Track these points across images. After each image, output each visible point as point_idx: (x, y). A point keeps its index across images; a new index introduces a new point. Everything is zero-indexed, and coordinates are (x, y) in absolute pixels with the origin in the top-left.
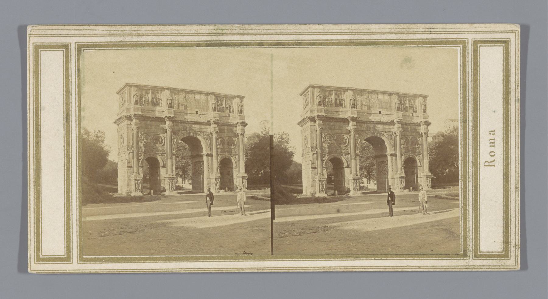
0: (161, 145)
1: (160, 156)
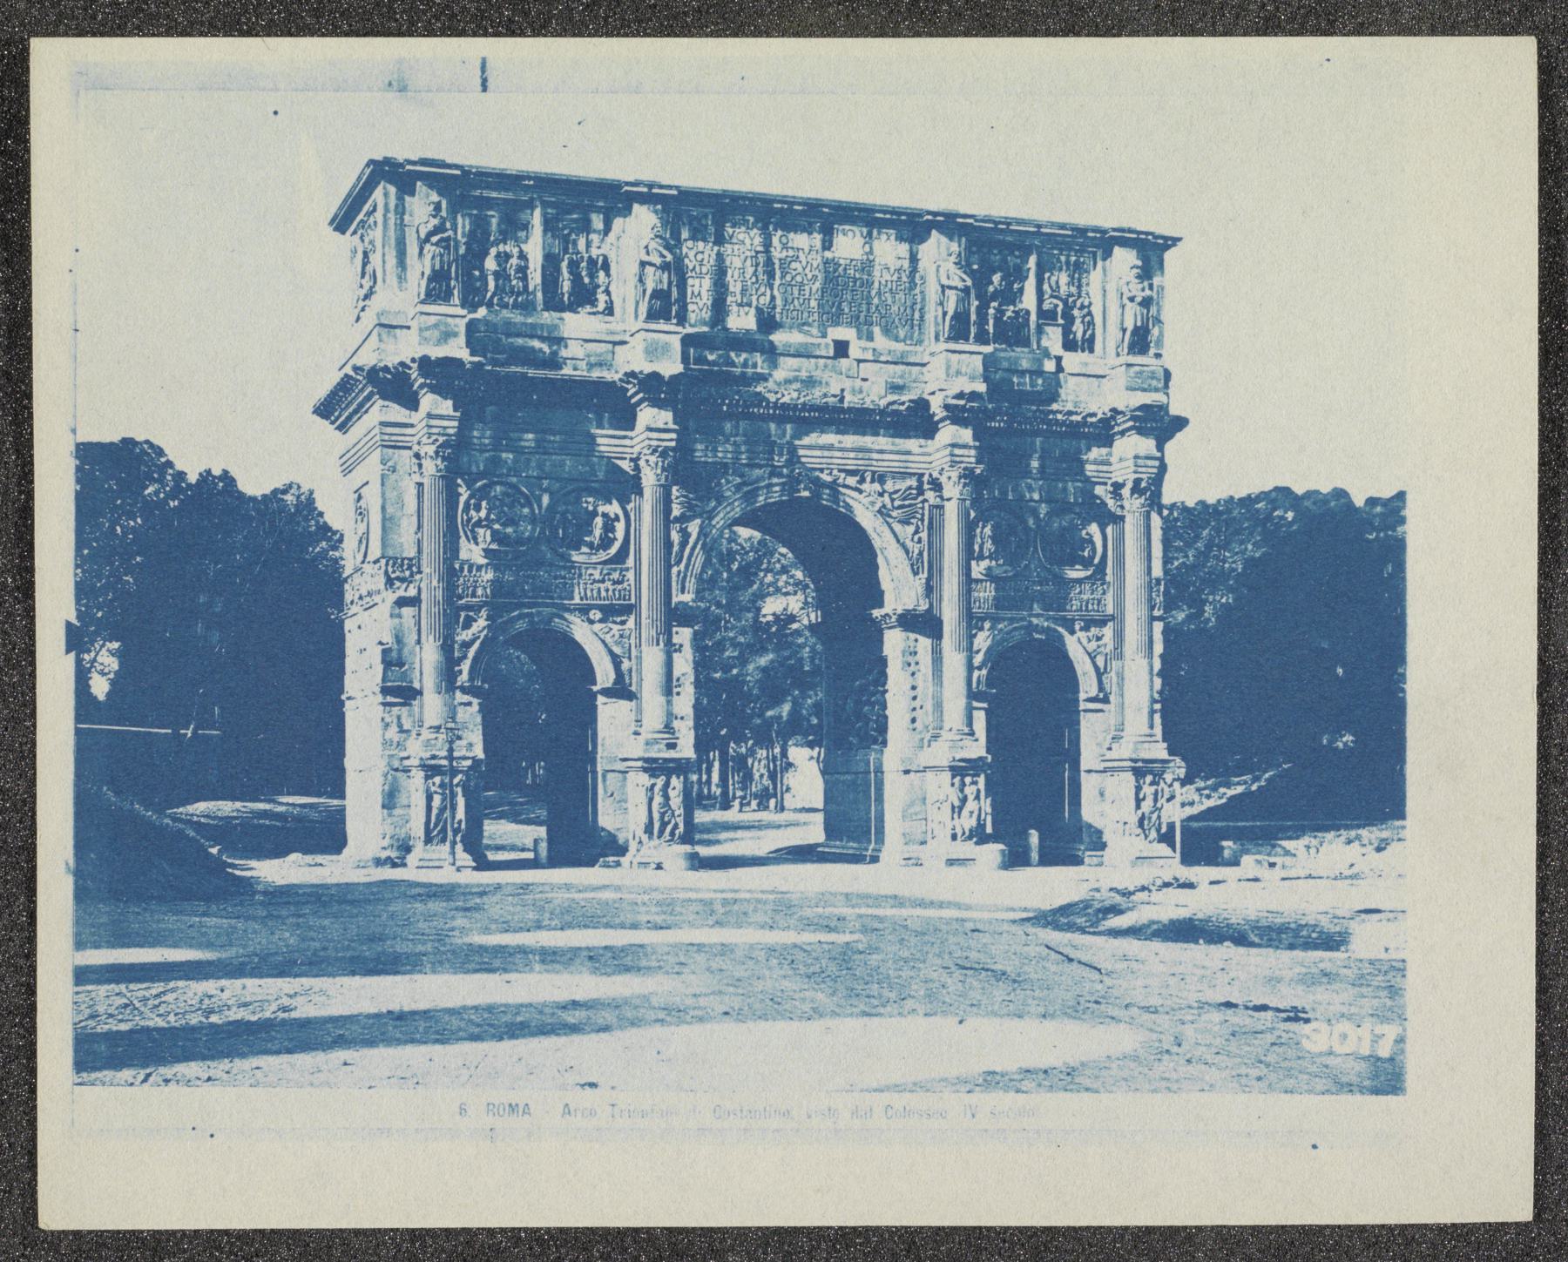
0: (603, 556)
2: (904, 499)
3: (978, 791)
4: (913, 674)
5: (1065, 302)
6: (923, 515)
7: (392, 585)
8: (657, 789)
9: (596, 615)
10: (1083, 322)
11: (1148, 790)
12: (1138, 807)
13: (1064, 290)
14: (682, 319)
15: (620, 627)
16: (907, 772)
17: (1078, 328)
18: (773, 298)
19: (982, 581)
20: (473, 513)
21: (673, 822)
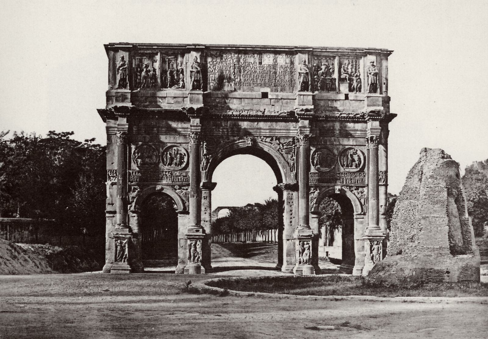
0: (180, 168)
1: (177, 191)
3: (309, 246)
4: (291, 206)
5: (350, 75)
6: (295, 151)
7: (110, 179)
8: (192, 245)
9: (177, 187)
10: (357, 81)
11: (375, 247)
12: (371, 252)
13: (350, 71)
14: (205, 89)
15: (185, 191)
16: (288, 240)
17: (355, 84)
18: (240, 79)
19: (317, 173)
20: (136, 154)
21: (198, 256)
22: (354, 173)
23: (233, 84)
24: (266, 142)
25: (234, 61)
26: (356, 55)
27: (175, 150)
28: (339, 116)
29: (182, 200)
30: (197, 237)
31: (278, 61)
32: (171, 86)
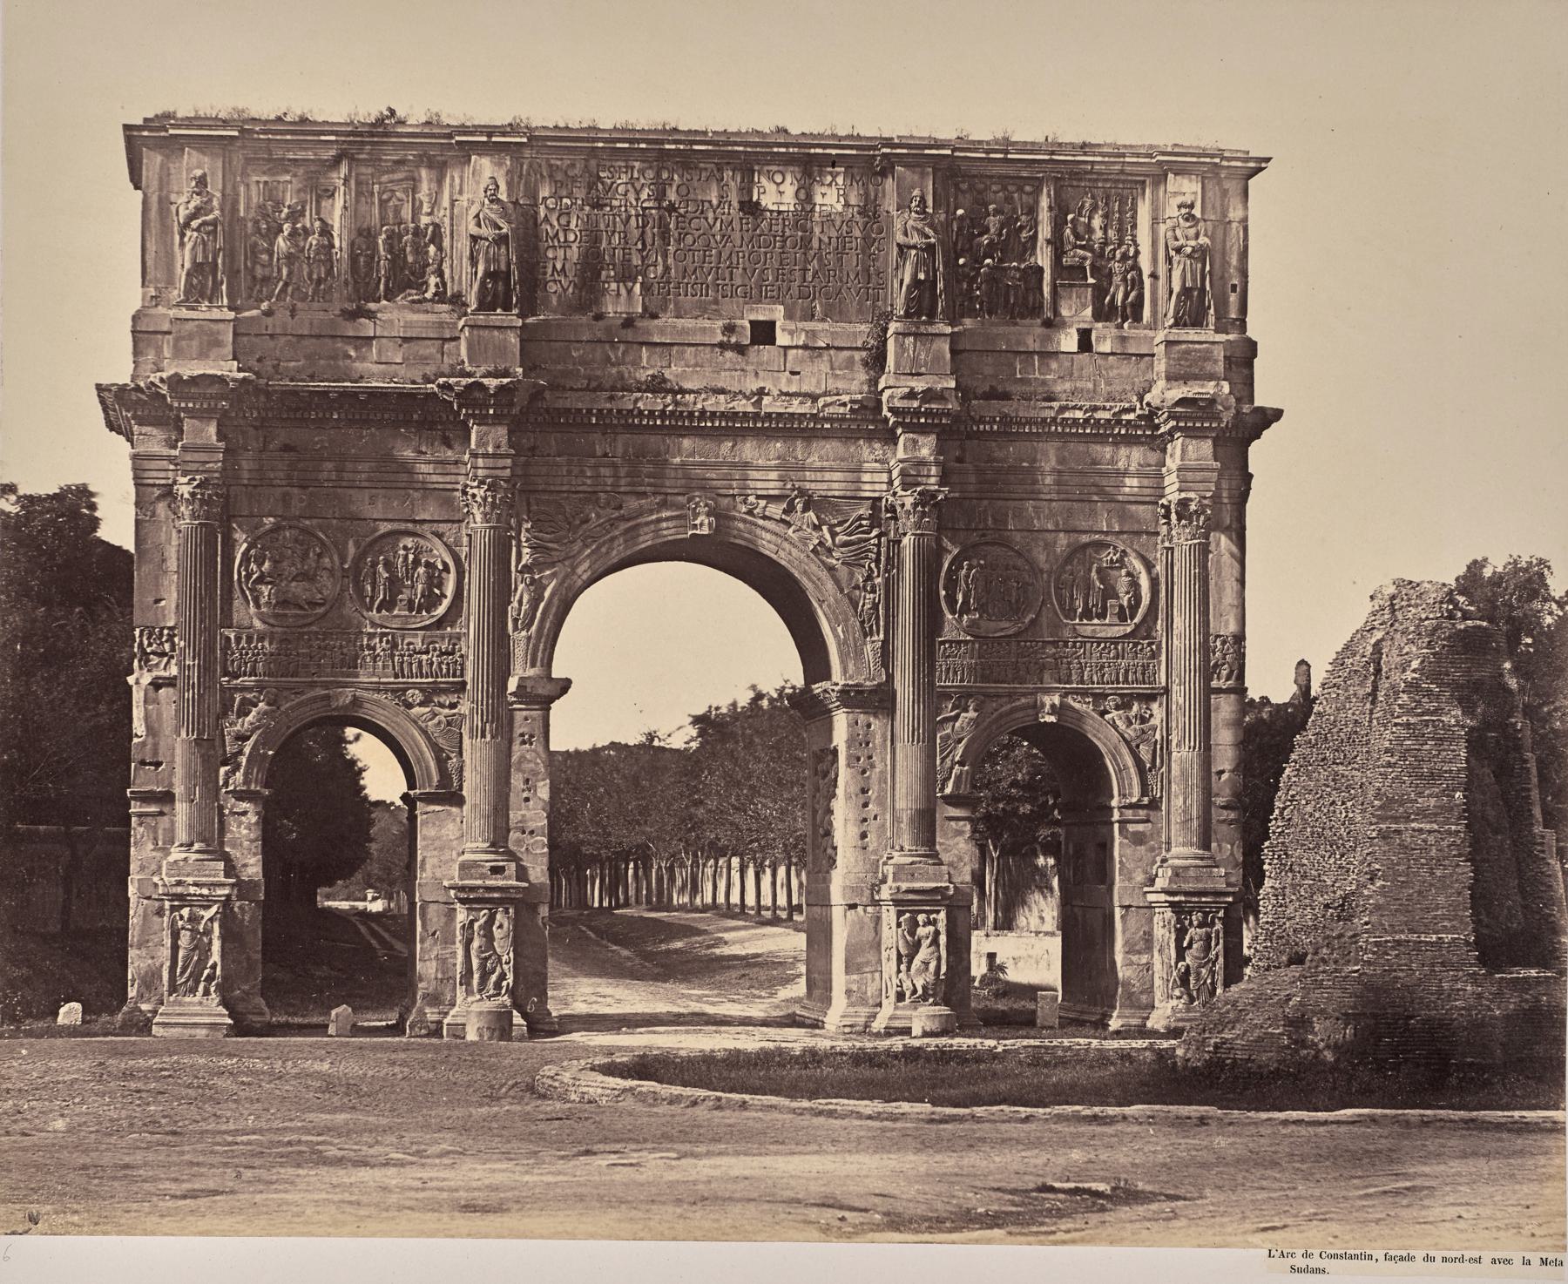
2: (850, 534)
3: (937, 933)
4: (864, 772)
6: (879, 553)
7: (148, 660)
8: (476, 925)
9: (415, 695)
10: (1124, 279)
12: (1181, 956)
15: (447, 711)
16: (853, 907)
18: (667, 269)
19: (966, 642)
20: (253, 566)
21: (498, 970)
22: (1114, 641)
23: (637, 288)
24: (765, 518)
25: (644, 196)
26: (1122, 172)
27: (405, 548)
28: (1054, 419)
29: (437, 750)
30: (496, 895)
31: (818, 199)
32: (389, 296)
